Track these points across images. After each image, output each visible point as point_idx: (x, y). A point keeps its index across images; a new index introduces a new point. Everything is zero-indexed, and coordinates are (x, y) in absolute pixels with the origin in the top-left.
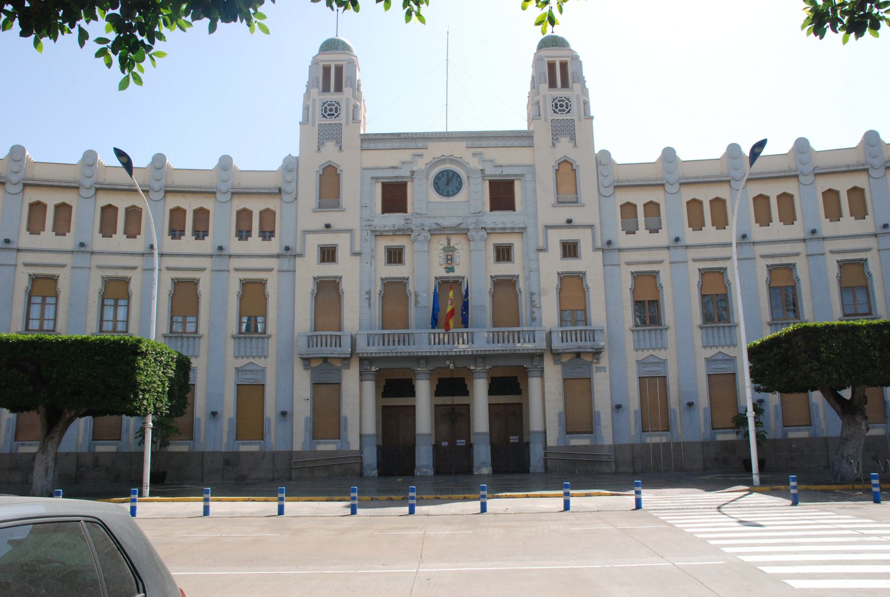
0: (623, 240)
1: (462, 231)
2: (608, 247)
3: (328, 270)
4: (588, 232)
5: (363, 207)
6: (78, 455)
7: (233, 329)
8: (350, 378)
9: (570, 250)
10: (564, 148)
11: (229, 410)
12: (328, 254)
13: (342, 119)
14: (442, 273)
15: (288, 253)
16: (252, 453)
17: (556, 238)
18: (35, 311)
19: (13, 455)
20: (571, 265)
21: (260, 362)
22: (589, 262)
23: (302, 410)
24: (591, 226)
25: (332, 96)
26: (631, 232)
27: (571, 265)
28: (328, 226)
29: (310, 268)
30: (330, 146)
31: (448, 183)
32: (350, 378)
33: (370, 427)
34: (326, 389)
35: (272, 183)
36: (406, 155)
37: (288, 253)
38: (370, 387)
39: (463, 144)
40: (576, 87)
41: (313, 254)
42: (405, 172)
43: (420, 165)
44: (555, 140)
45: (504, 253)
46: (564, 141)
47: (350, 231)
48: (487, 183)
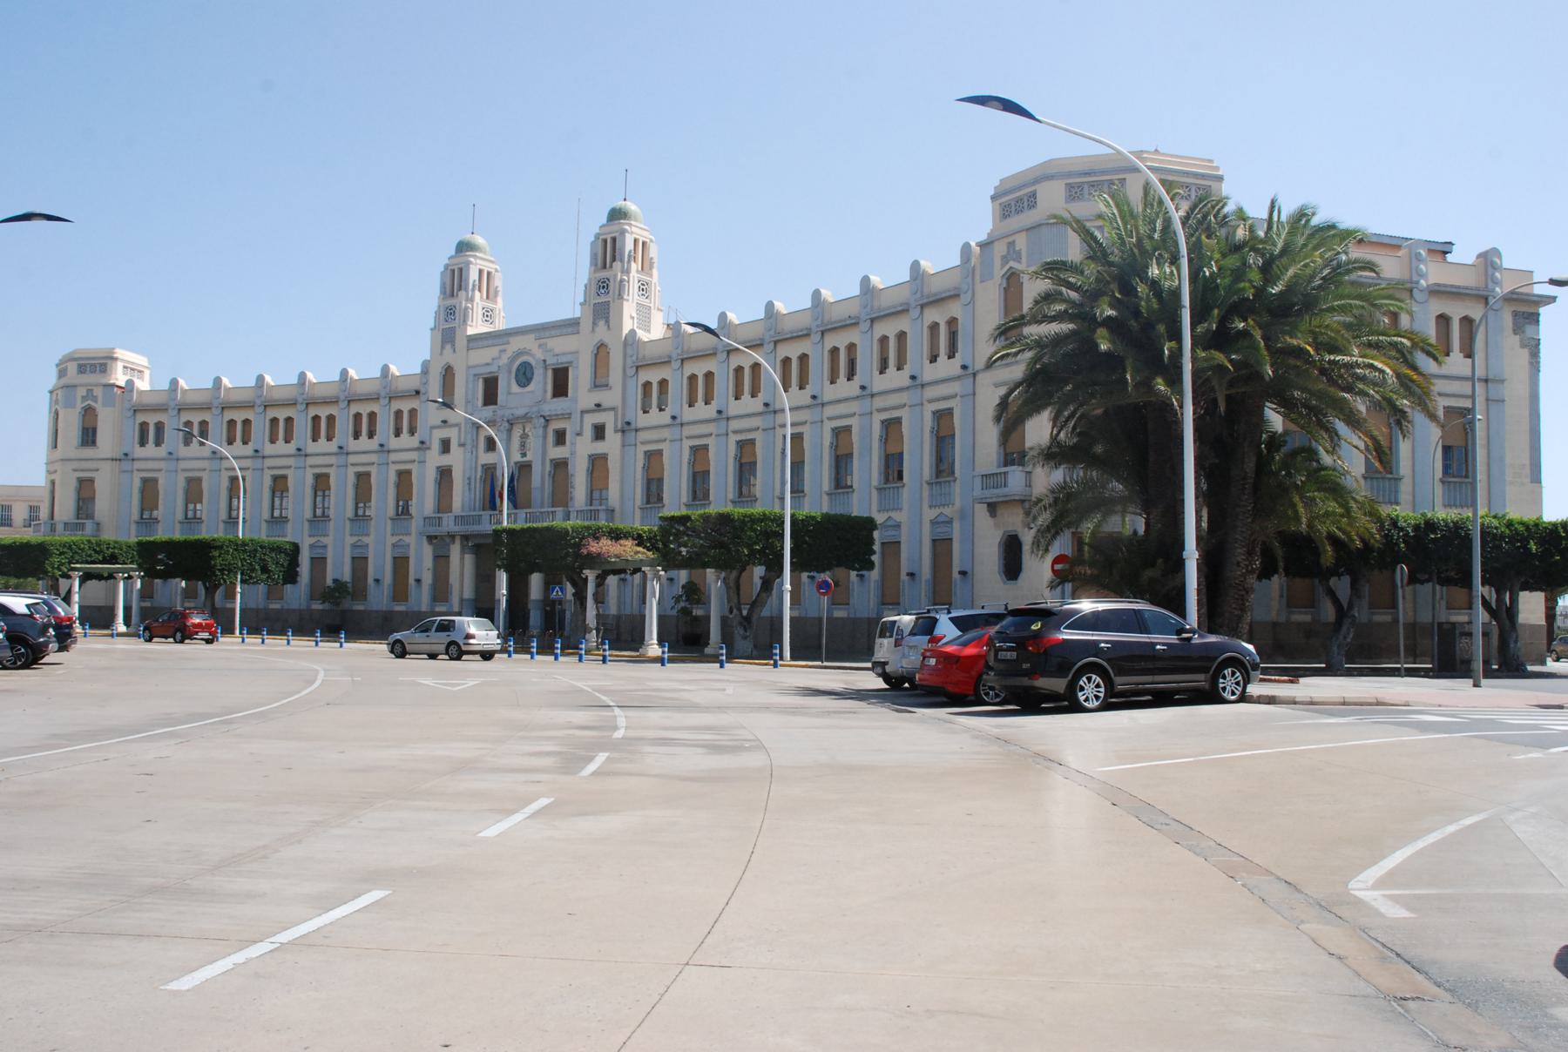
0: (642, 420)
1: (526, 418)
2: (626, 428)
3: (445, 460)
4: (612, 413)
5: (467, 402)
6: (300, 611)
7: (391, 512)
8: (455, 550)
9: (599, 432)
10: (602, 333)
11: (388, 579)
12: (446, 446)
13: (455, 324)
14: (517, 457)
15: (423, 446)
16: (400, 612)
17: (590, 420)
18: (277, 501)
19: (266, 609)
20: (600, 447)
21: (406, 539)
22: (611, 445)
23: (427, 579)
24: (613, 409)
25: (450, 302)
26: (645, 412)
27: (600, 447)
28: (444, 422)
29: (435, 459)
30: (448, 347)
31: (524, 375)
32: (455, 550)
33: (468, 593)
34: (441, 559)
35: (415, 385)
36: (494, 351)
37: (423, 446)
38: (469, 559)
39: (532, 336)
40: (617, 265)
41: (436, 446)
42: (493, 368)
43: (504, 360)
44: (594, 324)
45: (560, 438)
46: (602, 323)
47: (457, 425)
48: (550, 374)
